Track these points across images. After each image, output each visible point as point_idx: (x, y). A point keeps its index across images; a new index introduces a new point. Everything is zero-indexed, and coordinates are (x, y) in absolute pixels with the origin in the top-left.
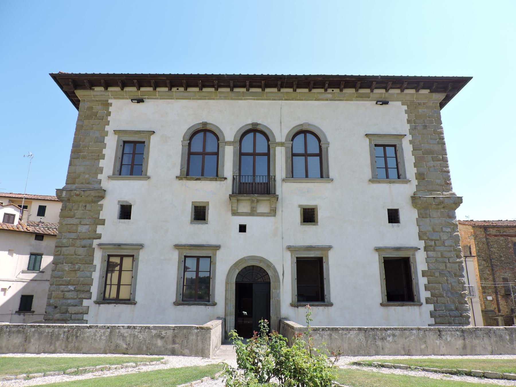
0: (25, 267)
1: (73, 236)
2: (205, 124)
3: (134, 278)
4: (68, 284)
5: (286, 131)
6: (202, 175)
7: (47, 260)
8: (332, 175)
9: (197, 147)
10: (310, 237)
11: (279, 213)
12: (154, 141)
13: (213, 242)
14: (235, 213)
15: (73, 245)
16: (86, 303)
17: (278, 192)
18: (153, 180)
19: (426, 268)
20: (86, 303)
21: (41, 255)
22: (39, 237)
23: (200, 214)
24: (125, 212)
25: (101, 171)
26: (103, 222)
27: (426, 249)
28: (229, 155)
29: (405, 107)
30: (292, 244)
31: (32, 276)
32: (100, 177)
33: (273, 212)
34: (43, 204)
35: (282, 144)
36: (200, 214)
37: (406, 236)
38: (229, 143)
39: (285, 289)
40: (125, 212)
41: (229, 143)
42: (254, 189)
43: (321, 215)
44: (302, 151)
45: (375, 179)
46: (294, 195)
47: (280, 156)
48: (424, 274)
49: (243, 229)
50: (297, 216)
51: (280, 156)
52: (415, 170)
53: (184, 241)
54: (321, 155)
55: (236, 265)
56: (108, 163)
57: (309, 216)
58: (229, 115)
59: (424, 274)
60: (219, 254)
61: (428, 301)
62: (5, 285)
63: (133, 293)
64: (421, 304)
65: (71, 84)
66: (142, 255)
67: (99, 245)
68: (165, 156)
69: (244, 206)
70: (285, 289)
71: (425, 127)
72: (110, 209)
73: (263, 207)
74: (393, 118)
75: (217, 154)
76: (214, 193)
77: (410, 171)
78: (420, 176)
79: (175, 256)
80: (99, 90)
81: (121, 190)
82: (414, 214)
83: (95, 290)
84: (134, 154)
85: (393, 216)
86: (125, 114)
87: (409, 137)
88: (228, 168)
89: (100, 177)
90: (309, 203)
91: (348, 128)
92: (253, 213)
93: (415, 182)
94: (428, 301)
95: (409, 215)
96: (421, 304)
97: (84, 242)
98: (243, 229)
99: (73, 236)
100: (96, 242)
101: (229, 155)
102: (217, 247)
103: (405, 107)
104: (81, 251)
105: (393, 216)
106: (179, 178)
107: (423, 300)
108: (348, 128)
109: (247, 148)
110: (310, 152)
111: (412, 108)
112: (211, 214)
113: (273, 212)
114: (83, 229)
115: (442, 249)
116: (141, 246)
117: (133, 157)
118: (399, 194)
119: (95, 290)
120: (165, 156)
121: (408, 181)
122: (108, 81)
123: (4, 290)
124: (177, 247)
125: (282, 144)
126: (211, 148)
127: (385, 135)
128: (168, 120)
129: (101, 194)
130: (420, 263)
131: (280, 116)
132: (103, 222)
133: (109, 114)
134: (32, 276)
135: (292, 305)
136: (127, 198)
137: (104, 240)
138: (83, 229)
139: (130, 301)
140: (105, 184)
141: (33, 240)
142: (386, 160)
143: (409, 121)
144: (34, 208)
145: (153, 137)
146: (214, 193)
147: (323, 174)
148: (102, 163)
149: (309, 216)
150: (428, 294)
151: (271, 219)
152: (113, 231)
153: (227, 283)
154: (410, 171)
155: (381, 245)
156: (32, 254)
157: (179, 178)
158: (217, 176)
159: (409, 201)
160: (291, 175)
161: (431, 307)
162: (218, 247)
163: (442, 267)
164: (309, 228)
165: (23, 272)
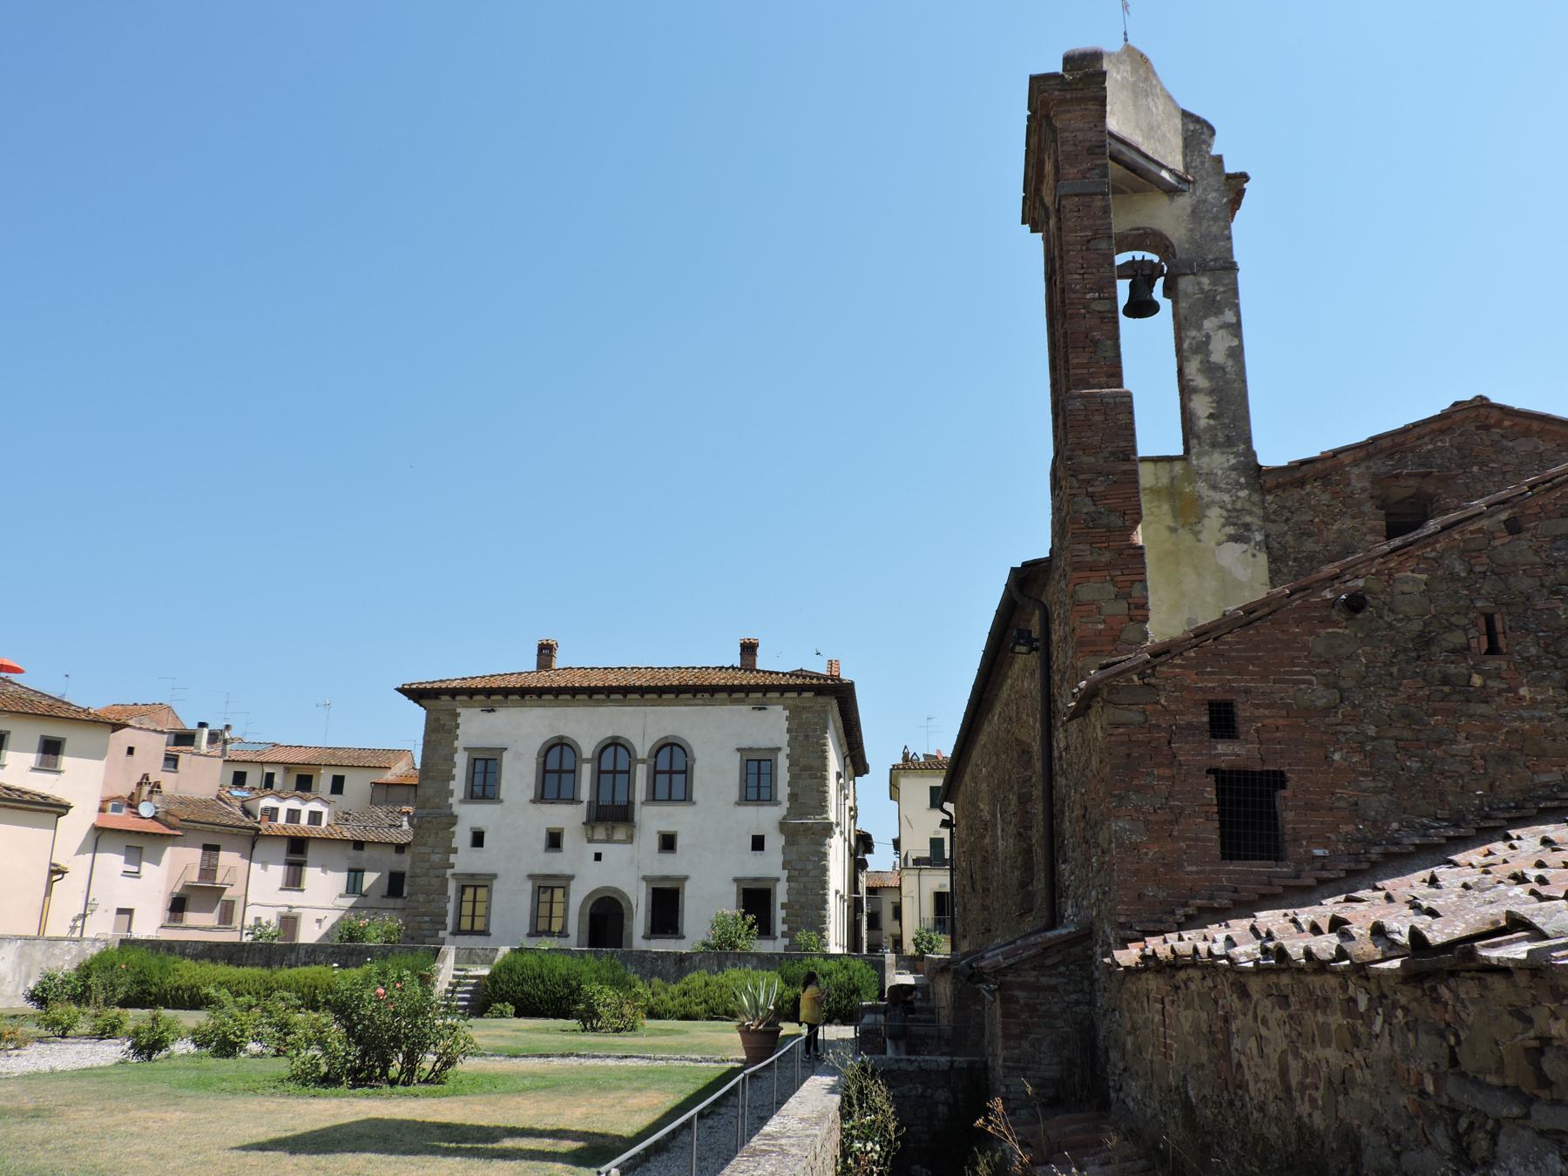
0: (343, 890)
1: (427, 865)
2: (561, 738)
3: (488, 908)
4: (424, 915)
5: (649, 745)
6: (558, 799)
7: (369, 879)
8: (696, 796)
9: (553, 764)
10: (667, 866)
11: (636, 840)
12: (506, 756)
13: (567, 871)
14: (590, 841)
15: (426, 875)
16: (442, 934)
17: (636, 818)
18: (506, 804)
19: (785, 900)
20: (442, 934)
21: (363, 871)
22: (359, 845)
23: (554, 841)
24: (478, 839)
25: (451, 793)
26: (455, 851)
27: (789, 879)
28: (586, 771)
29: (787, 713)
30: (648, 873)
31: (350, 901)
32: (451, 800)
33: (630, 839)
34: (339, 772)
35: (643, 761)
36: (554, 841)
37: (770, 864)
38: (587, 761)
39: (639, 921)
40: (478, 839)
41: (587, 761)
42: (611, 816)
43: (680, 842)
44: (667, 768)
45: (745, 800)
46: (652, 819)
47: (641, 774)
48: (783, 906)
49: (598, 857)
50: (655, 842)
51: (641, 774)
52: (788, 790)
53: (537, 871)
54: (687, 772)
55: (590, 896)
56: (458, 786)
57: (668, 843)
58: (588, 727)
59: (783, 906)
60: (573, 885)
61: (784, 935)
62: (321, 914)
63: (487, 924)
64: (775, 938)
65: (416, 694)
66: (496, 885)
67: (453, 875)
68: (518, 777)
69: (600, 833)
70: (639, 921)
71: (807, 737)
72: (462, 837)
73: (620, 834)
74: (770, 727)
75: (573, 771)
76: (568, 817)
77: (783, 790)
78: (793, 797)
79: (528, 886)
80: (445, 698)
81: (471, 816)
82: (782, 841)
83: (450, 921)
84: (486, 772)
85: (758, 843)
86: (475, 728)
87: (787, 750)
88: (585, 793)
89: (451, 800)
90: (667, 828)
91: (718, 739)
92: (609, 840)
93: (787, 804)
94: (784, 935)
95: (775, 842)
96: (775, 938)
97: (438, 872)
98: (598, 857)
99: (427, 865)
100: (449, 872)
101: (586, 771)
102: (571, 877)
103: (787, 713)
104: (435, 881)
105: (758, 843)
106: (533, 801)
107: (778, 934)
108: (718, 739)
109: (607, 764)
110: (673, 769)
111: (795, 714)
112: (566, 841)
113: (630, 839)
114: (436, 858)
115: (805, 879)
116: (494, 876)
117: (485, 778)
118: (766, 819)
119: (450, 921)
120: (518, 777)
121: (777, 803)
122: (454, 693)
123: (319, 921)
124: (531, 877)
125: (643, 761)
126: (567, 765)
127: (760, 749)
128: (520, 734)
129: (453, 820)
130: (781, 895)
131: (643, 727)
132: (455, 851)
133: (457, 726)
134: (350, 901)
135: (644, 937)
136: (479, 824)
137: (457, 869)
138: (436, 858)
139: (485, 933)
140: (458, 809)
141: (352, 852)
142: (755, 778)
143: (789, 731)
144: (324, 782)
145: (505, 754)
146: (568, 817)
147: (687, 798)
148: (452, 785)
149: (668, 843)
150: (785, 928)
151: (628, 846)
152: (465, 860)
153: (580, 914)
154: (783, 790)
155: (740, 875)
156: (350, 871)
157: (533, 801)
158: (574, 800)
159: (777, 825)
160: (653, 798)
161: (786, 941)
162: (571, 877)
163: (803, 899)
164: (667, 857)
165: (341, 896)
